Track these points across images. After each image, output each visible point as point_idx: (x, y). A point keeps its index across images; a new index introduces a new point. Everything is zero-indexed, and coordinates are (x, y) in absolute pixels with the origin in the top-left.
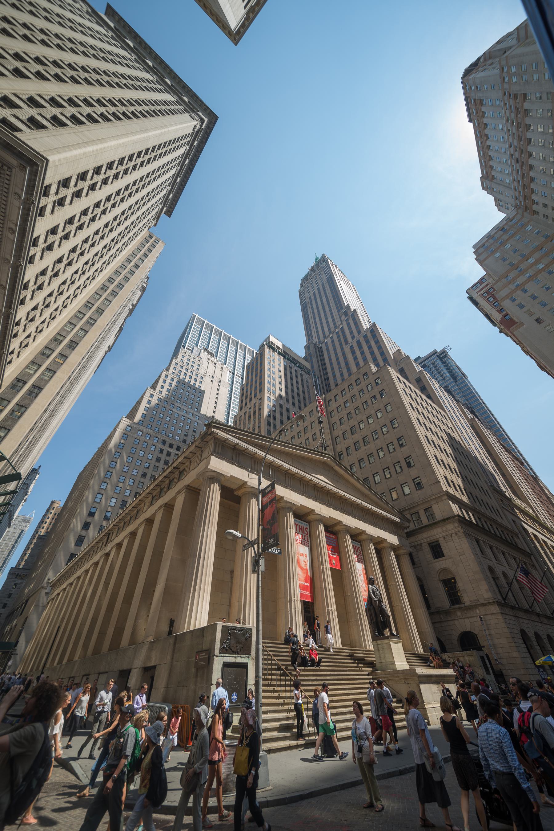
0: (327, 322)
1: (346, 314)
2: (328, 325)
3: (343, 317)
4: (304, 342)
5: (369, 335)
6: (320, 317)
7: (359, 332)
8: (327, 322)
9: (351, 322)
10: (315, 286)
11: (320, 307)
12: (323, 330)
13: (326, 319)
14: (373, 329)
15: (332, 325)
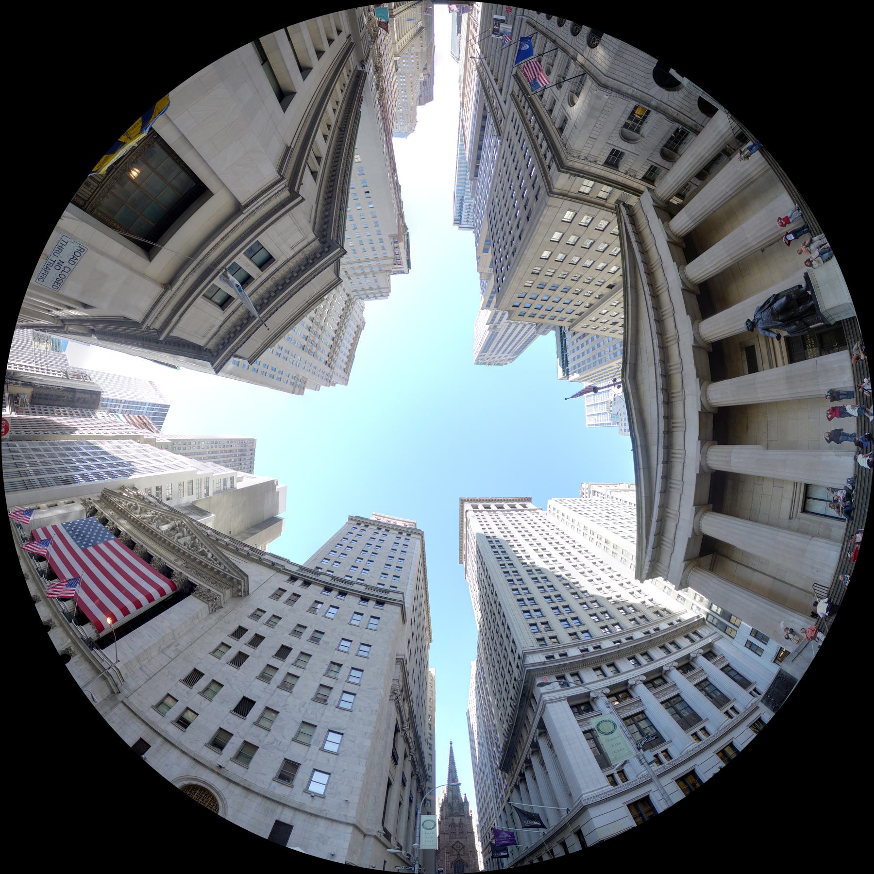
0: (513, 332)
1: (495, 327)
2: (514, 329)
3: (499, 327)
4: (540, 338)
5: (493, 305)
6: (515, 338)
7: (496, 314)
8: (513, 332)
9: (497, 320)
10: (498, 356)
11: (507, 343)
12: (521, 330)
13: (511, 334)
14: (487, 306)
15: (512, 327)
